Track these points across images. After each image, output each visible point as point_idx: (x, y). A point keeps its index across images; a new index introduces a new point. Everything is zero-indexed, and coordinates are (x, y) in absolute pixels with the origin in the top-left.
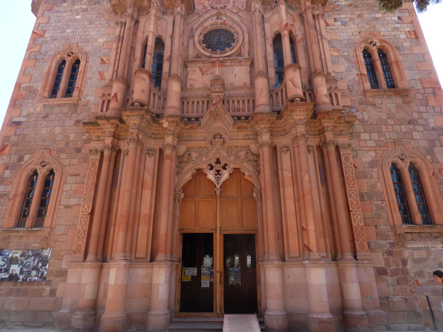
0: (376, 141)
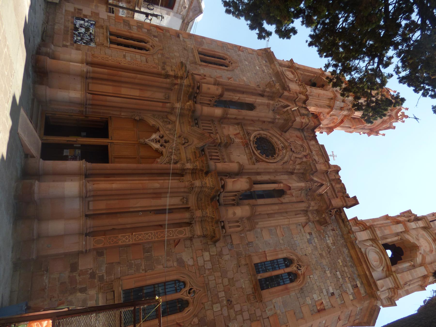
0: (204, 266)
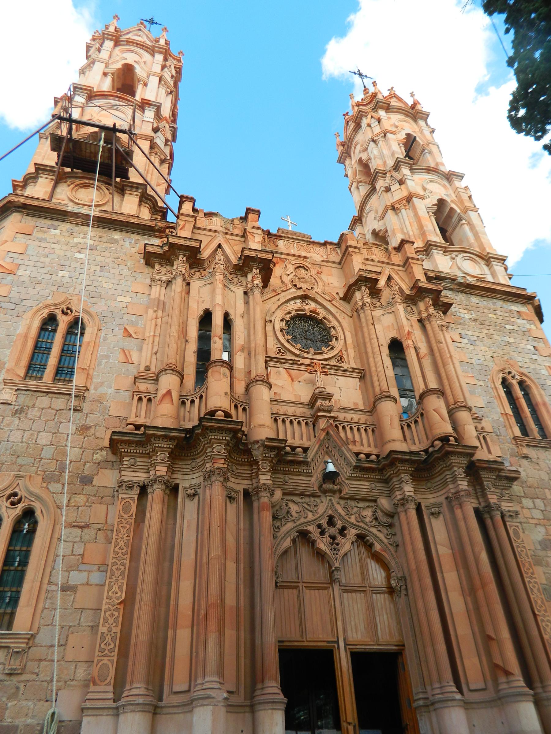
0: (542, 511)
